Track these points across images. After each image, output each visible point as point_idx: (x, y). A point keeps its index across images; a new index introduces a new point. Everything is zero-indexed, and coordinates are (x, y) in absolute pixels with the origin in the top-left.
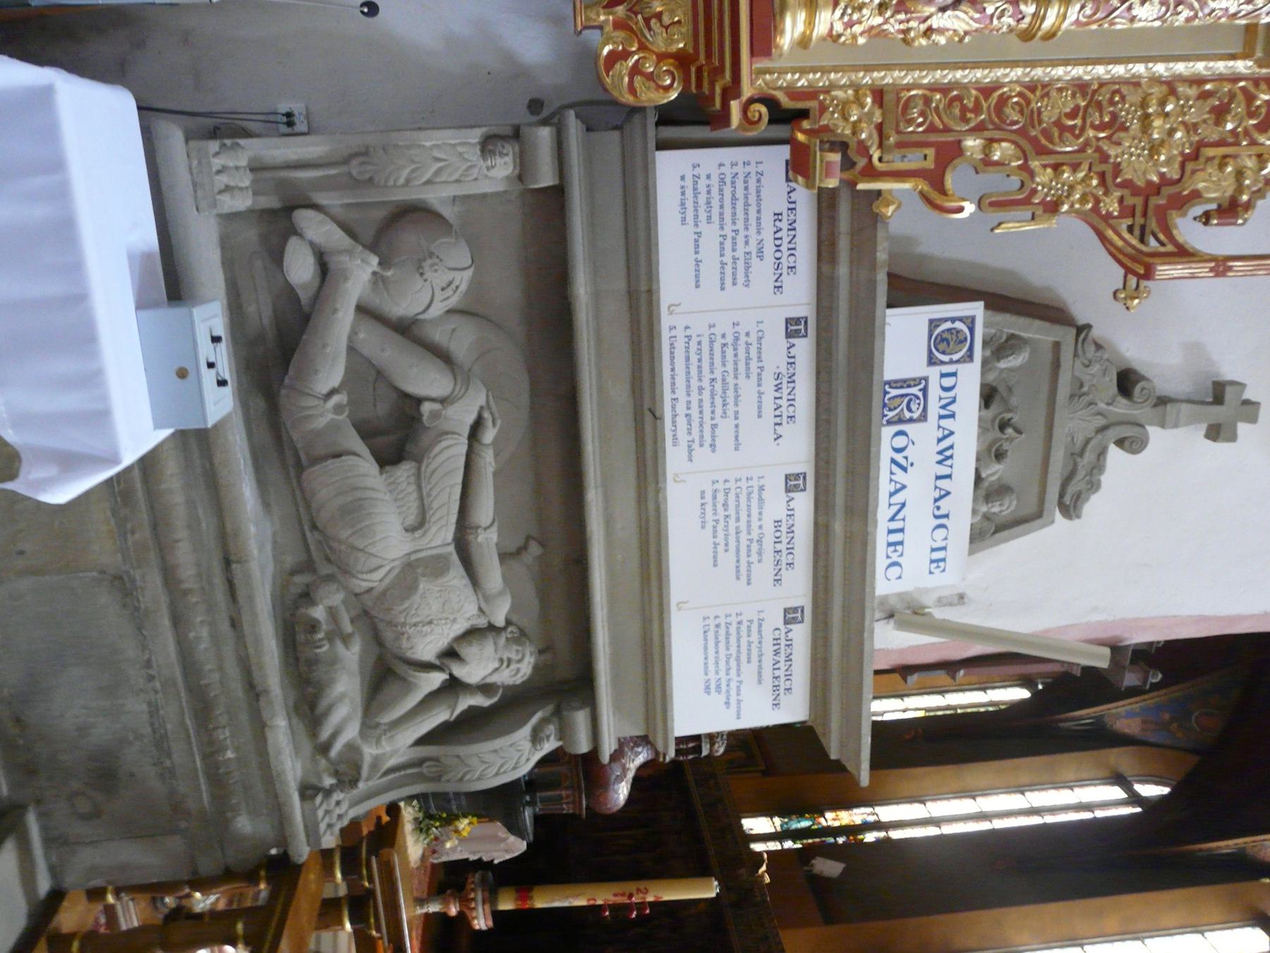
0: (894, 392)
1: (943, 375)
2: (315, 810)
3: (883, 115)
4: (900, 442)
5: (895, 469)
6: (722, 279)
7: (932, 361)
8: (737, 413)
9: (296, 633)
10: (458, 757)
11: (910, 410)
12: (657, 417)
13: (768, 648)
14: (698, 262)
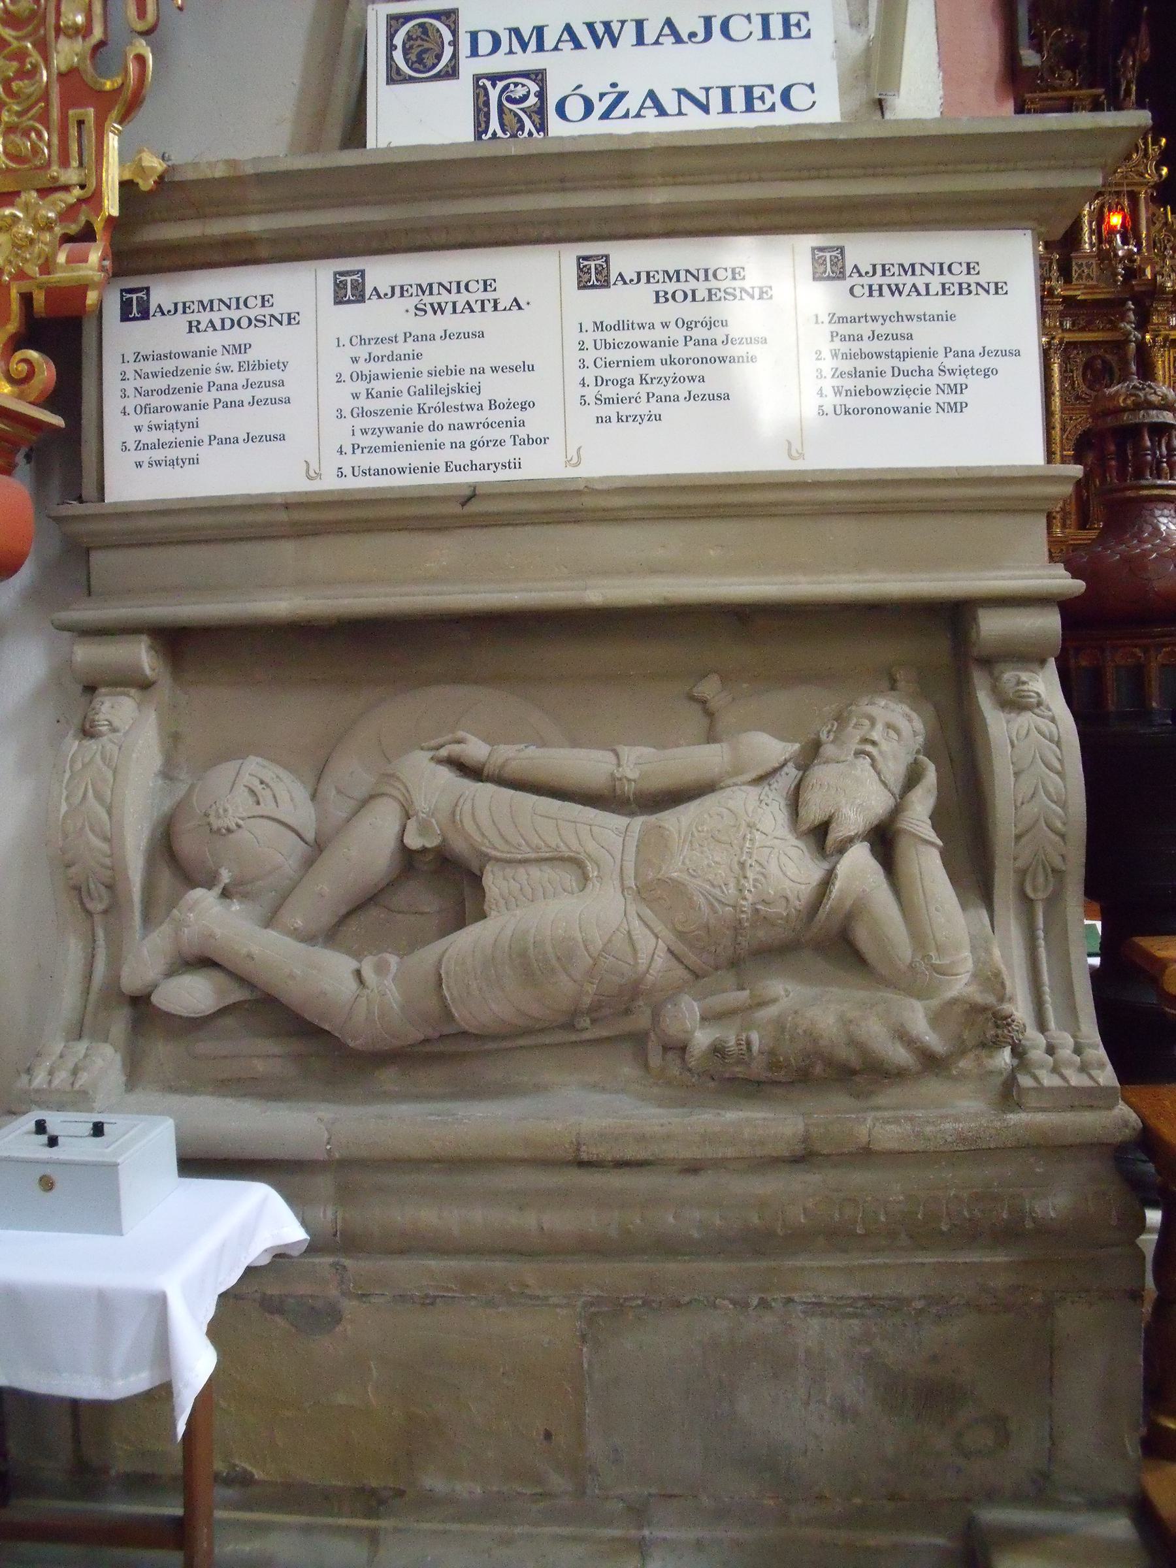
0: (494, 125)
1: (474, 52)
2: (1040, 1089)
3: (27, 189)
4: (575, 108)
5: (620, 111)
6: (274, 402)
7: (452, 73)
8: (473, 371)
9: (733, 1077)
10: (1018, 837)
11: (525, 98)
12: (472, 495)
13: (888, 304)
14: (249, 438)
